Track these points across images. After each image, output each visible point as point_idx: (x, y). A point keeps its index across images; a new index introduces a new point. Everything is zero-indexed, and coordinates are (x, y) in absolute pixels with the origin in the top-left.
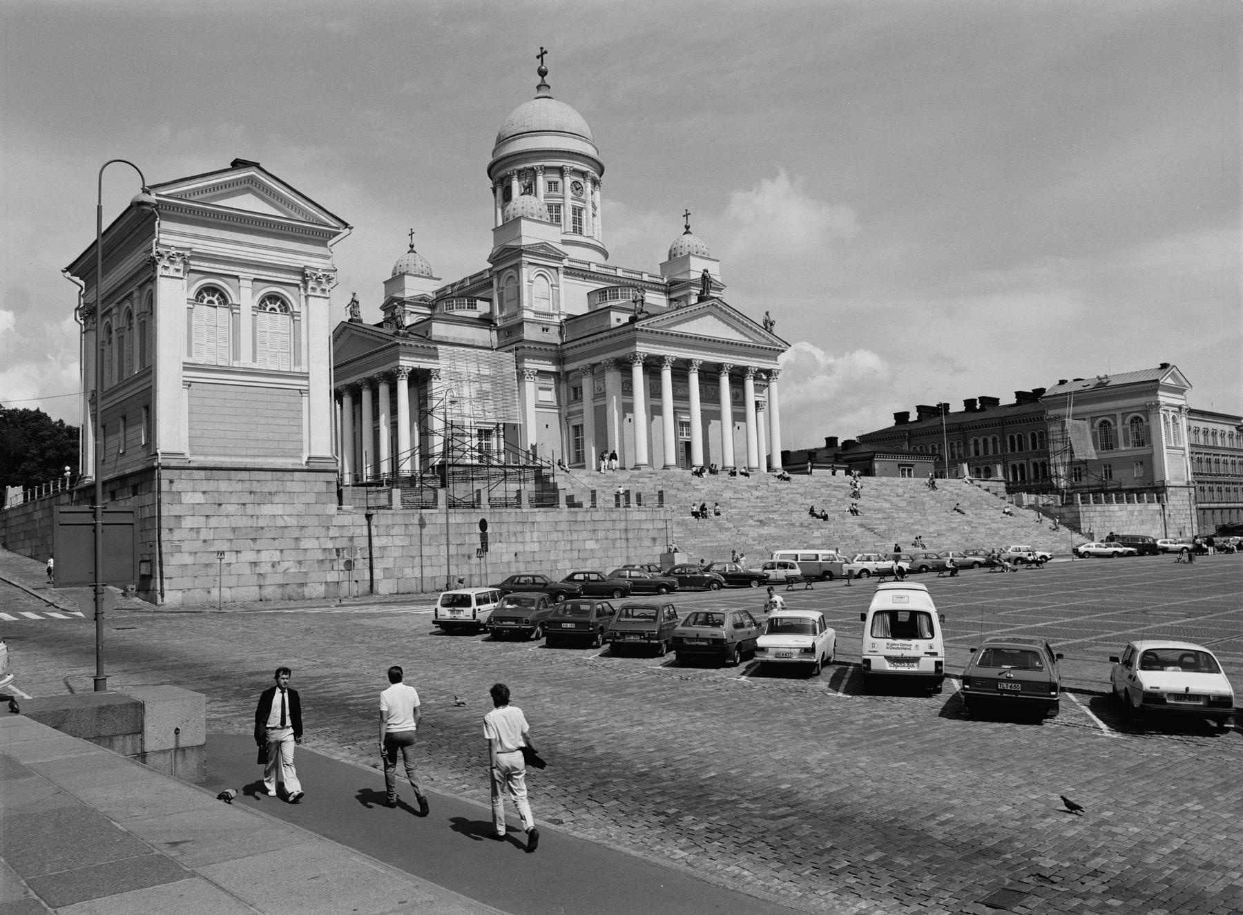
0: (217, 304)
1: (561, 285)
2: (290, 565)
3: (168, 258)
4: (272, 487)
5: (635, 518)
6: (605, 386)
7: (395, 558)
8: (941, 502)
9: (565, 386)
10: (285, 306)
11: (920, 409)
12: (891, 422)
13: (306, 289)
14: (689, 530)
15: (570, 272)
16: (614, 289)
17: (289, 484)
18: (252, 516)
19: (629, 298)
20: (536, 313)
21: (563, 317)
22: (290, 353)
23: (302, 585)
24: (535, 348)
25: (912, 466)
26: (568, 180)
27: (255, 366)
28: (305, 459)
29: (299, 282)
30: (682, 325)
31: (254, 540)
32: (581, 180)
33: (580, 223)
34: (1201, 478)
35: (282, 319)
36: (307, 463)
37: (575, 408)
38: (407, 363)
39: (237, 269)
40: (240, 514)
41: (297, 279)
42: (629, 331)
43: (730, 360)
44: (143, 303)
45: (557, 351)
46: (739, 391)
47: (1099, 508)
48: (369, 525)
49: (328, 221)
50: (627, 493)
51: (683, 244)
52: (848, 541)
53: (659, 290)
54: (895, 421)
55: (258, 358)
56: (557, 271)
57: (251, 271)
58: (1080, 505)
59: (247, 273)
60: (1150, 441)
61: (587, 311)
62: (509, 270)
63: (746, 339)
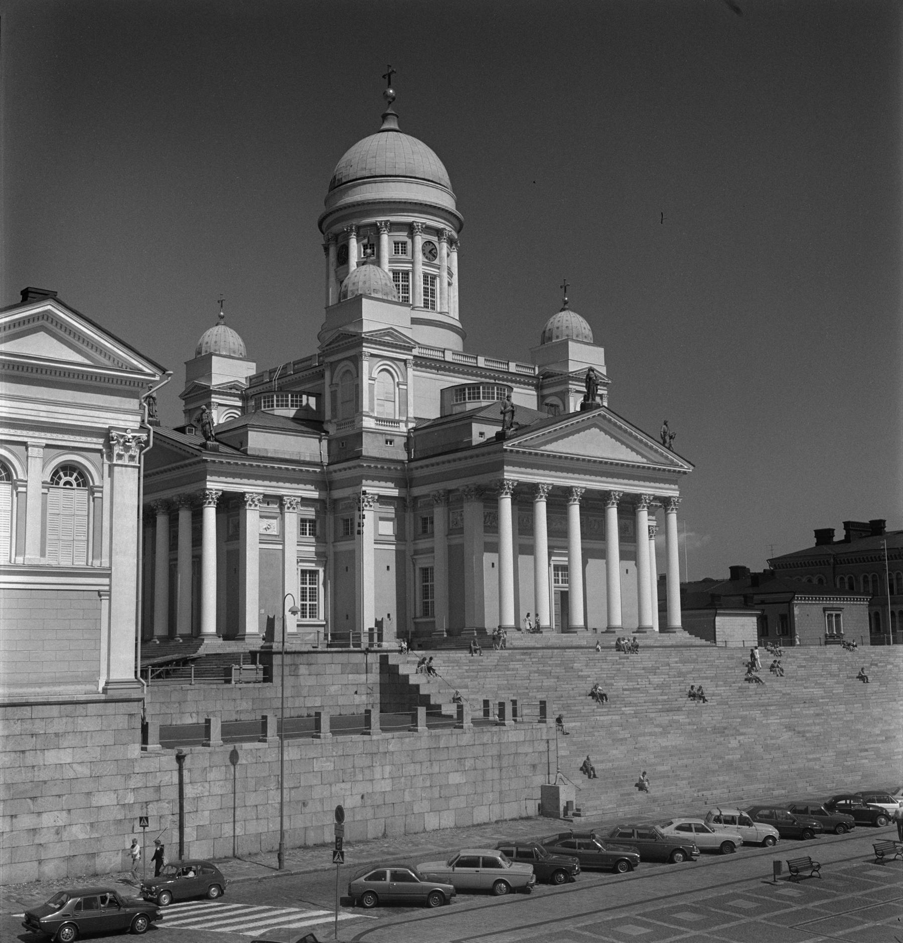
2: (79, 832)
4: (58, 726)
5: (510, 740)
6: (462, 520)
9: (412, 515)
10: (83, 479)
11: (847, 525)
12: (811, 542)
14: (575, 744)
15: (422, 362)
16: (475, 387)
17: (80, 721)
18: (33, 767)
19: (493, 398)
20: (377, 419)
21: (411, 425)
22: (88, 541)
23: (93, 855)
24: (376, 467)
25: (840, 609)
27: (44, 561)
28: (102, 685)
31: (33, 799)
32: (434, 239)
35: (81, 495)
36: (105, 690)
37: (423, 544)
39: (25, 433)
41: (97, 443)
45: (403, 470)
49: (141, 366)
53: (529, 384)
54: (815, 540)
56: (405, 364)
57: (43, 434)
61: (439, 416)
63: (644, 460)
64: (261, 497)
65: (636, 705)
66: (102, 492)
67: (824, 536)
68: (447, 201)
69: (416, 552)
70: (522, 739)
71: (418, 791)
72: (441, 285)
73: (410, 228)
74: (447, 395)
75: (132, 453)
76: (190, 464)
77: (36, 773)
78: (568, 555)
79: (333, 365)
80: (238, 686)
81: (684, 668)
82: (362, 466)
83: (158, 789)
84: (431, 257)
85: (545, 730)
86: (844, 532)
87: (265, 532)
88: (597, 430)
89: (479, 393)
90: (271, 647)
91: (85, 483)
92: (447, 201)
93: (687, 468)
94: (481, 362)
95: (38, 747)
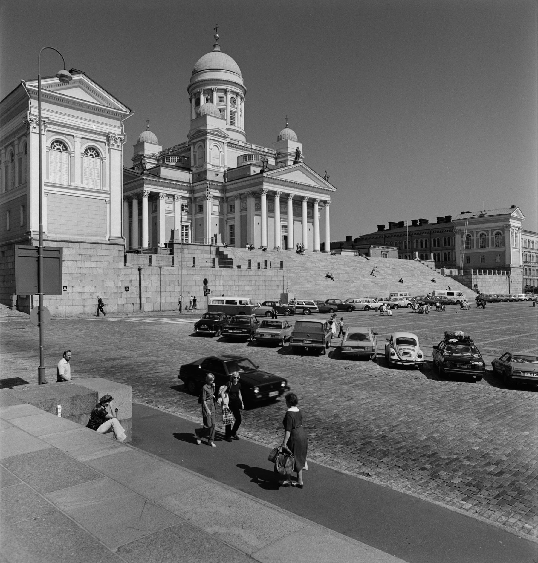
0: (62, 150)
1: (226, 151)
3: (36, 122)
4: (90, 252)
6: (246, 205)
7: (152, 292)
8: (407, 271)
10: (98, 155)
11: (390, 224)
12: (376, 230)
13: (109, 145)
14: (293, 281)
15: (230, 145)
17: (99, 251)
18: (80, 268)
20: (213, 165)
21: (226, 169)
22: (100, 180)
25: (387, 252)
26: (229, 96)
27: (82, 186)
28: (108, 238)
29: (105, 141)
30: (283, 175)
32: (235, 96)
33: (234, 118)
34: (526, 264)
35: (97, 160)
36: (109, 240)
37: (230, 216)
38: (148, 189)
39: (73, 131)
42: (260, 178)
43: (308, 195)
44: (20, 146)
46: (311, 211)
47: (480, 277)
48: (140, 274)
50: (266, 261)
51: (284, 133)
52: (367, 290)
54: (378, 229)
55: (84, 181)
57: (80, 133)
58: (473, 275)
59: (78, 134)
60: (504, 244)
62: (199, 143)
63: (317, 185)
64: (166, 195)
65: (315, 271)
66: (106, 160)
67: (381, 227)
68: (240, 81)
69: (228, 219)
70: (274, 275)
71: (234, 292)
73: (225, 91)
74: (240, 159)
75: (118, 144)
76: (137, 181)
77: (82, 270)
78: (287, 221)
79: (195, 144)
80: (160, 255)
81: (333, 261)
82: (206, 183)
83: (131, 281)
84: (234, 103)
85: (282, 272)
86: (389, 226)
87: (167, 209)
88: (300, 171)
89: (253, 158)
90: (173, 241)
91: (99, 156)
93: (334, 189)
94: (253, 146)
95: (82, 260)
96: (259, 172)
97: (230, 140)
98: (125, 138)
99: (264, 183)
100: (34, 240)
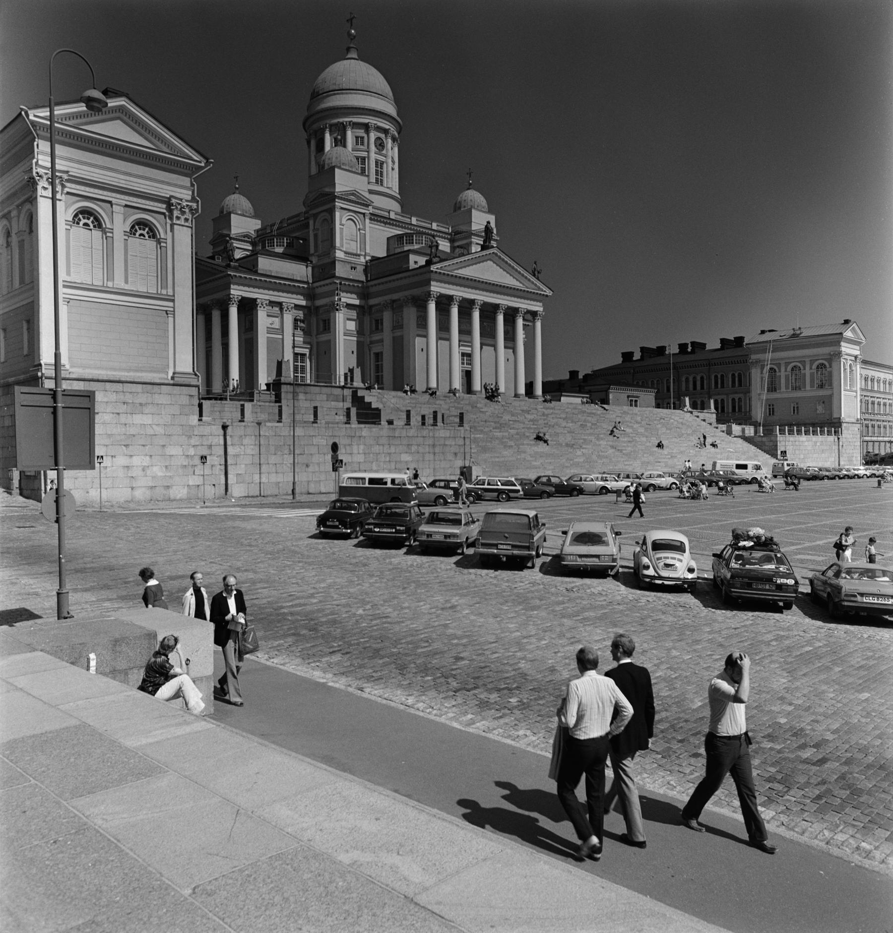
0: (92, 227)
1: (367, 229)
3: (47, 180)
4: (142, 398)
5: (441, 435)
6: (403, 319)
7: (246, 465)
8: (670, 429)
10: (153, 234)
11: (643, 349)
12: (619, 360)
13: (171, 218)
15: (375, 218)
16: (410, 235)
17: (156, 396)
18: (126, 424)
19: (422, 243)
20: (346, 253)
21: (368, 258)
22: (157, 277)
23: (168, 487)
25: (638, 397)
26: (373, 135)
28: (170, 374)
29: (164, 211)
30: (464, 269)
31: (126, 446)
32: (382, 136)
33: (382, 176)
34: (867, 416)
35: (151, 244)
36: (173, 378)
37: (376, 337)
39: (109, 194)
40: (114, 422)
41: (162, 207)
43: (505, 301)
44: (21, 219)
46: (510, 328)
47: (791, 438)
49: (191, 154)
50: (435, 413)
52: (604, 460)
53: (445, 238)
54: (622, 359)
55: (130, 279)
56: (364, 216)
57: (122, 197)
58: (779, 435)
60: (831, 385)
61: (385, 255)
62: (325, 214)
63: (521, 285)
64: (268, 302)
66: (166, 243)
67: (627, 356)
68: (391, 110)
69: (372, 342)
71: (382, 464)
72: (387, 168)
73: (366, 127)
76: (220, 278)
77: (128, 429)
78: (471, 346)
79: (315, 216)
80: (258, 403)
81: (546, 412)
83: (210, 447)
84: (381, 148)
85: (463, 431)
86: (640, 354)
87: (270, 326)
88: (492, 263)
90: (280, 380)
91: (154, 236)
92: (391, 110)
93: (549, 292)
94: (414, 221)
96: (424, 263)
97: (375, 210)
98: (198, 206)
99: (432, 283)
100: (46, 378)
